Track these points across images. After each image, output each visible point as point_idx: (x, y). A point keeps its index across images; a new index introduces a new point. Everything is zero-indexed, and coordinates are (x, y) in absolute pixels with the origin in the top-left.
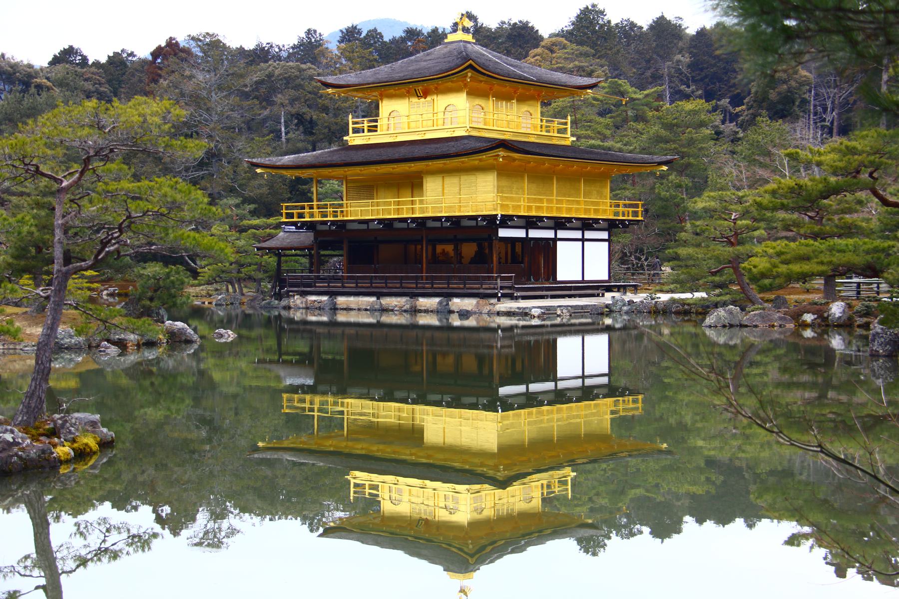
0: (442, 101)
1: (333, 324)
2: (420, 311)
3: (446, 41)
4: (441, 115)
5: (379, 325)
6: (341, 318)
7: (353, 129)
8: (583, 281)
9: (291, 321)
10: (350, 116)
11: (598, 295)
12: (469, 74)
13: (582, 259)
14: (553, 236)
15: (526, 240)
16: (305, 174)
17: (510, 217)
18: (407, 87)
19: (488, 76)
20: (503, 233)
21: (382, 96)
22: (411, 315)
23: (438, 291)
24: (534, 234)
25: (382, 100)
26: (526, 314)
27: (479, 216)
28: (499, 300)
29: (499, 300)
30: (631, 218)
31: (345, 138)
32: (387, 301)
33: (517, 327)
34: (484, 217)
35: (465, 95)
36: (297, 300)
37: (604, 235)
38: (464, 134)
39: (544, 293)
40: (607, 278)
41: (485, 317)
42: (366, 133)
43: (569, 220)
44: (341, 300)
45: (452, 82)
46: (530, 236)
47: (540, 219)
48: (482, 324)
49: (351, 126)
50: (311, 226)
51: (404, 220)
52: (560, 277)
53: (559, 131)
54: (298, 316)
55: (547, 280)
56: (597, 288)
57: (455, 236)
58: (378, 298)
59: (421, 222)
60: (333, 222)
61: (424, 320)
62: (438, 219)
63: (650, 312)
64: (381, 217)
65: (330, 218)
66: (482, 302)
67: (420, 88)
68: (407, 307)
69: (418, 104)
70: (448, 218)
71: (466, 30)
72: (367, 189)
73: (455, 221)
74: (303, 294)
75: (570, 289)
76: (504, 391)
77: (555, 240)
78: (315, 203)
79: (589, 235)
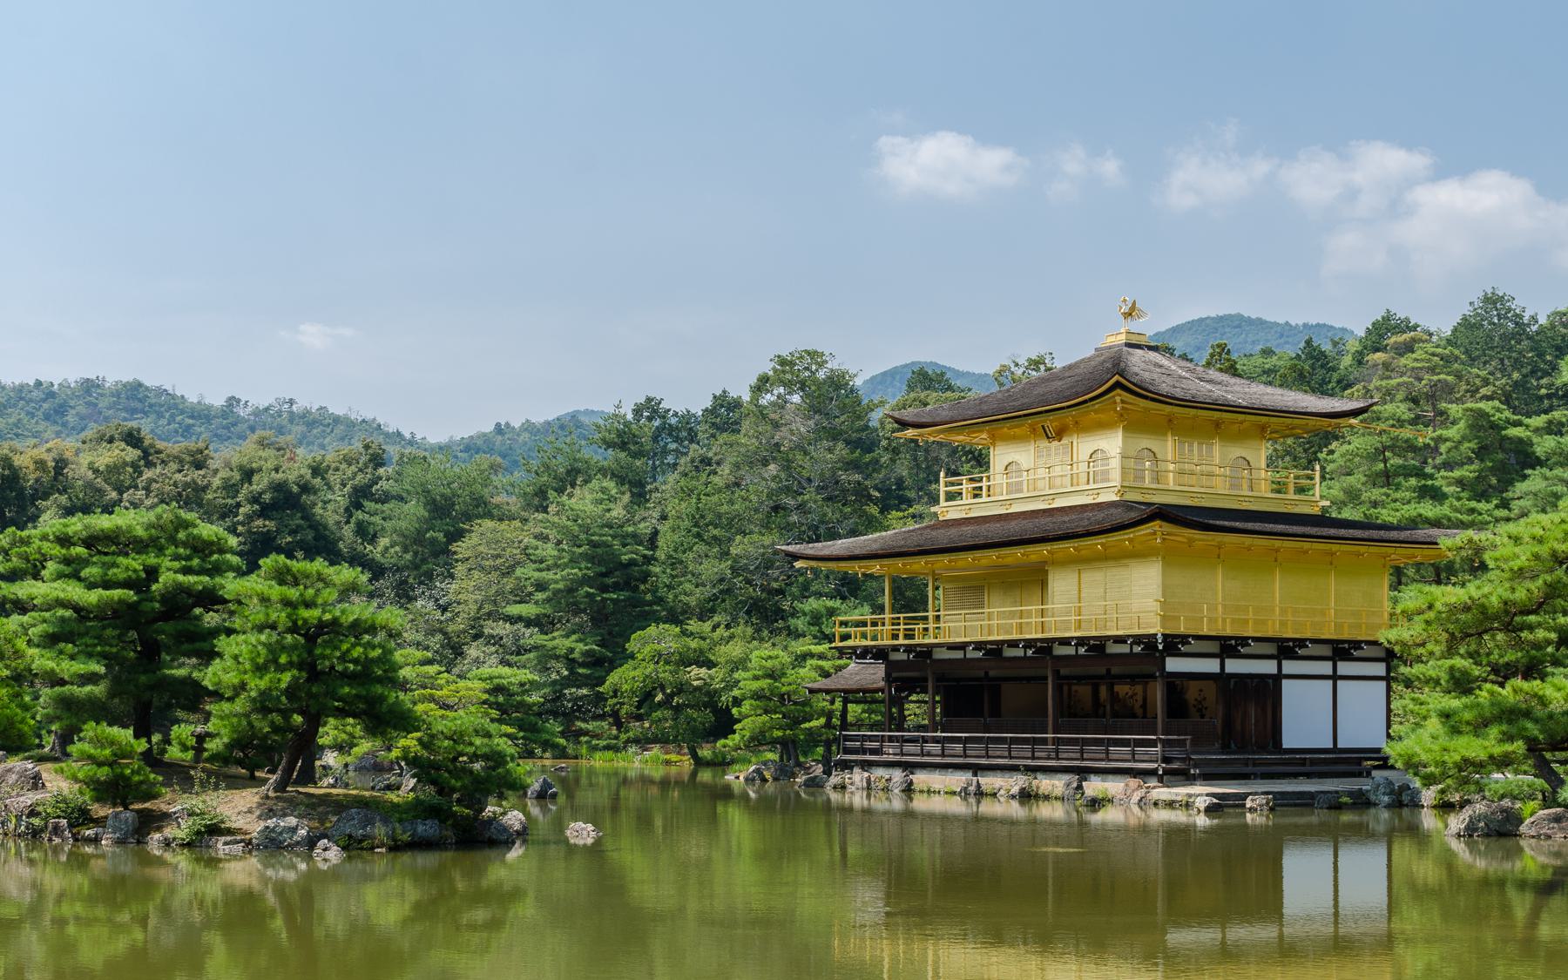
0: (1084, 446)
1: (909, 814)
2: (1037, 797)
4: (1083, 467)
5: (977, 819)
6: (920, 804)
7: (947, 493)
8: (1335, 749)
9: (848, 810)
10: (942, 474)
11: (1360, 775)
12: (1118, 399)
14: (1275, 671)
15: (1221, 678)
16: (919, 565)
17: (1184, 639)
20: (1174, 665)
21: (994, 439)
22: (1022, 803)
23: (1065, 763)
24: (1234, 666)
25: (994, 444)
28: (1161, 780)
31: (933, 509)
32: (989, 781)
34: (1138, 639)
35: (1120, 433)
36: (858, 776)
37: (1379, 669)
38: (1112, 497)
39: (1250, 769)
41: (1136, 809)
42: (967, 499)
43: (1301, 643)
44: (921, 779)
45: (1096, 412)
47: (1243, 641)
48: (1133, 821)
49: (943, 489)
50: (880, 654)
51: (1013, 644)
52: (1288, 742)
53: (1301, 490)
54: (858, 800)
55: (1262, 748)
56: (1359, 761)
57: (1108, 671)
58: (975, 775)
59: (1044, 648)
60: (909, 649)
61: (1046, 811)
62: (1065, 642)
63: (1375, 805)
64: (979, 638)
65: (901, 641)
66: (1133, 782)
67: (1051, 423)
68: (1015, 790)
69: (1049, 449)
70: (1081, 641)
72: (973, 590)
73: (1097, 646)
74: (866, 765)
75: (1303, 762)
76: (1178, 937)
77: (1278, 678)
78: (887, 616)
79: (1344, 668)
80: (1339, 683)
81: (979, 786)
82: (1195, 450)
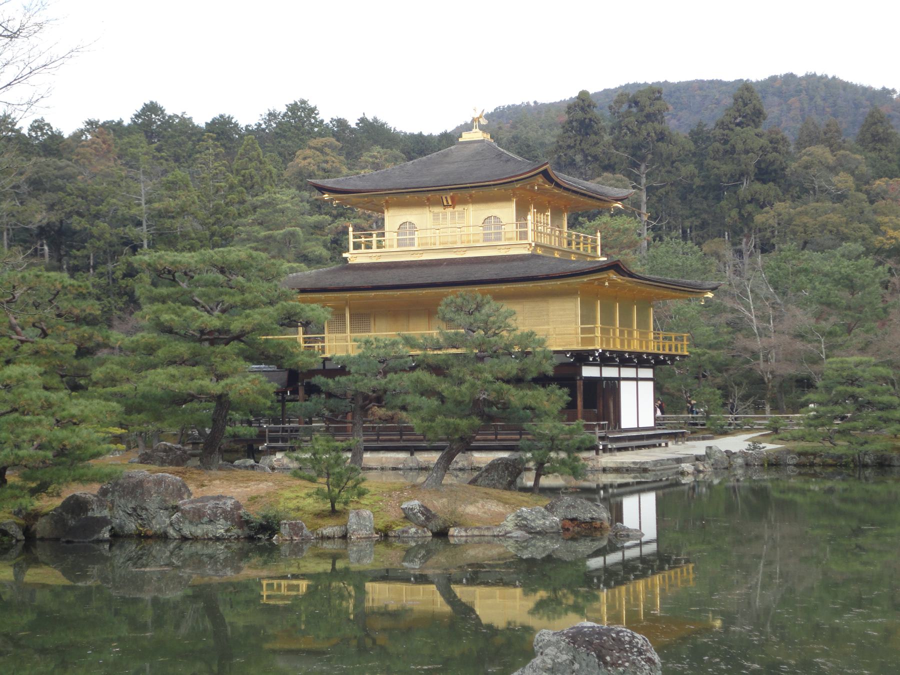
3: (460, 140)
8: (638, 429)
10: (351, 229)
13: (637, 405)
18: (437, 195)
19: (558, 185)
20: (589, 372)
21: (389, 205)
24: (610, 372)
26: (645, 470)
27: (568, 351)
28: (597, 454)
29: (597, 454)
30: (679, 352)
31: (344, 255)
33: (611, 486)
37: (648, 373)
40: (652, 425)
42: (375, 249)
46: (604, 375)
52: (623, 426)
58: (412, 454)
67: (447, 197)
69: (445, 215)
71: (483, 128)
80: (640, 383)
81: (418, 462)
82: (541, 218)
